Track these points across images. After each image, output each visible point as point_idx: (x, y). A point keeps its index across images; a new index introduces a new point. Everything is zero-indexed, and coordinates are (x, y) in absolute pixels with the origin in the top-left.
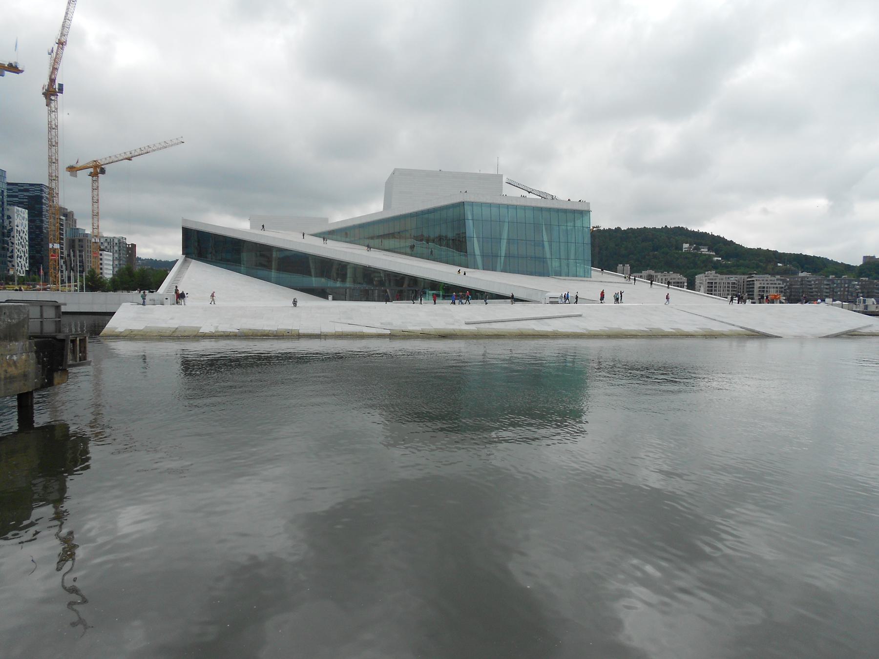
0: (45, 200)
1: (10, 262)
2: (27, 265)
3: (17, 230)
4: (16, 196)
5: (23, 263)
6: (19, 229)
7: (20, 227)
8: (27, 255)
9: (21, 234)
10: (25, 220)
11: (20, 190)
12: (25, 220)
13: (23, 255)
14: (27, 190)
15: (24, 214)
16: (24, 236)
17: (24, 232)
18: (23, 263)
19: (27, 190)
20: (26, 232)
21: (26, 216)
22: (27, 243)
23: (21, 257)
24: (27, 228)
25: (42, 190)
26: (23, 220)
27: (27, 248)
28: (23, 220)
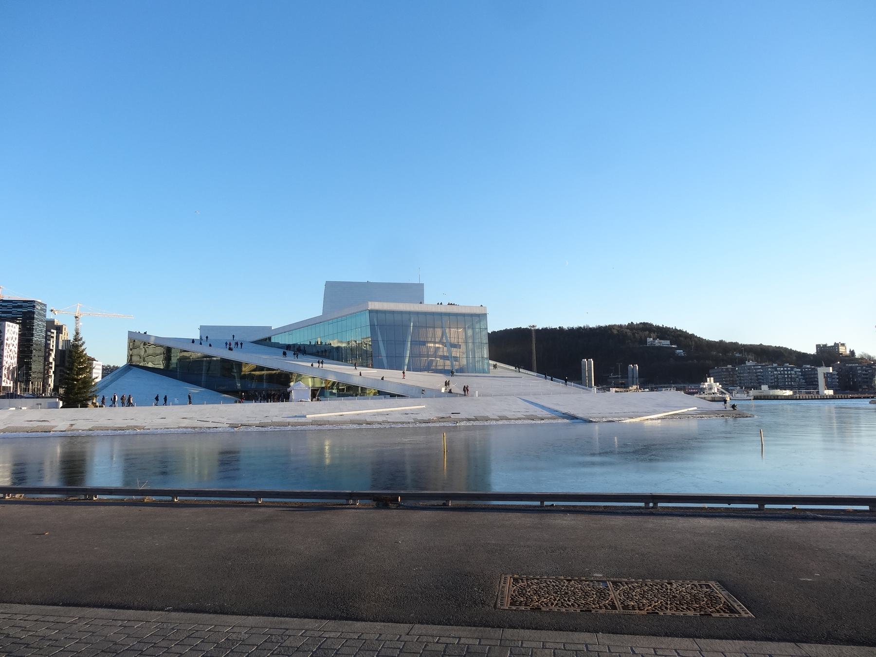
0: (37, 315)
3: (7, 344)
6: (9, 342)
7: (10, 340)
10: (16, 333)
12: (16, 333)
14: (21, 307)
15: (15, 328)
16: (13, 348)
17: (13, 345)
20: (15, 345)
22: (16, 355)
24: (17, 342)
25: (34, 306)
26: (14, 334)
28: (14, 334)
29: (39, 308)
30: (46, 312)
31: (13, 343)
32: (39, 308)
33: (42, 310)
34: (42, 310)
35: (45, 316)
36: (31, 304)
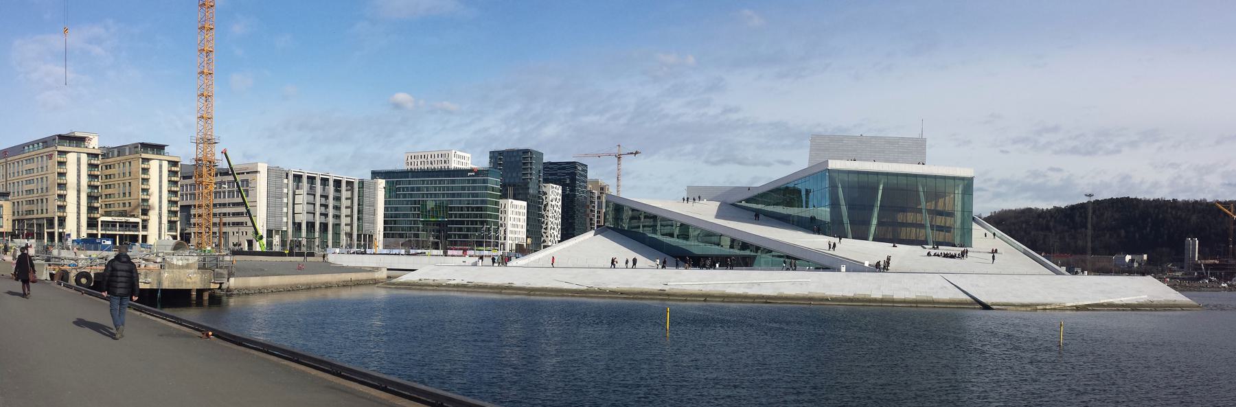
1: (545, 233)
2: (559, 236)
4: (556, 174)
5: (556, 233)
6: (553, 203)
7: (554, 201)
8: (559, 227)
9: (555, 208)
11: (559, 169)
13: (555, 226)
14: (564, 168)
16: (557, 209)
18: (556, 233)
19: (564, 168)
21: (560, 191)
23: (554, 230)
24: (560, 203)
25: (576, 168)
27: (560, 220)
29: (581, 169)
30: (586, 173)
31: (557, 203)
32: (581, 169)
33: (583, 170)
34: (583, 170)
35: (586, 177)
36: (573, 165)
